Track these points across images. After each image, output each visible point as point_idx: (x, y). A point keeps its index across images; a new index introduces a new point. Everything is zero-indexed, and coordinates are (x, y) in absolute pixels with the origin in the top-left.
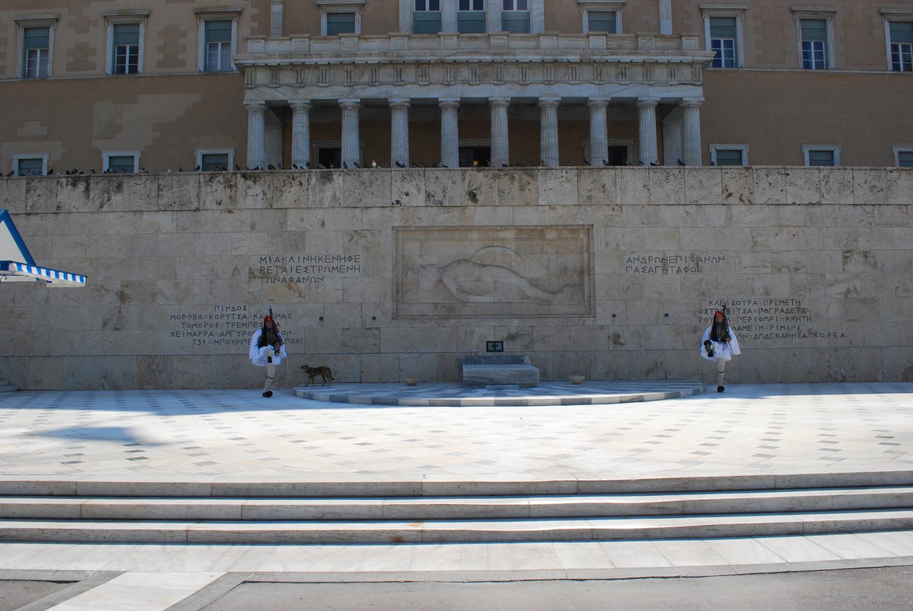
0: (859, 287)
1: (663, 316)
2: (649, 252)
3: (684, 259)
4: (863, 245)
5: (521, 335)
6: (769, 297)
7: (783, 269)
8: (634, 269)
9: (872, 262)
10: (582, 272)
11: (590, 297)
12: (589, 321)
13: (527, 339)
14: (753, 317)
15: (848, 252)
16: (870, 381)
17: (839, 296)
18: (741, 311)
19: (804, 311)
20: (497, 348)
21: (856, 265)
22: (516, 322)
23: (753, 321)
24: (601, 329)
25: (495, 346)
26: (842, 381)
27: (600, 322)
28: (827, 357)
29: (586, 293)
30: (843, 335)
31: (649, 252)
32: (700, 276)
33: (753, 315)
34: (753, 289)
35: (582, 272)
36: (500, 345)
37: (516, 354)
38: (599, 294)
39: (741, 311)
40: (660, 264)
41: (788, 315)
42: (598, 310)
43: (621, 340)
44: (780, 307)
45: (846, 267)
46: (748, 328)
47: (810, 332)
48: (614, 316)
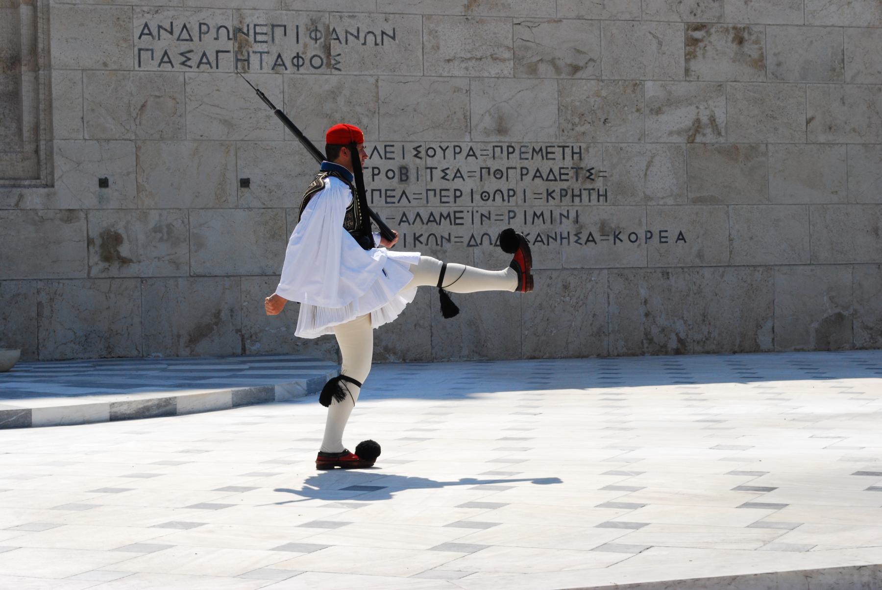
0: (721, 119)
1: (235, 184)
2: (199, 9)
3: (291, 32)
4: (734, 11)
6: (506, 140)
7: (542, 68)
8: (158, 55)
9: (755, 55)
10: (14, 61)
11: (36, 129)
12: (34, 198)
14: (466, 190)
15: (699, 27)
16: (742, 351)
17: (675, 139)
18: (438, 174)
19: (590, 175)
21: (718, 62)
23: (466, 198)
26: (678, 352)
27: (65, 201)
28: (643, 292)
29: (27, 119)
30: (681, 237)
31: (199, 9)
32: (333, 79)
33: (467, 185)
34: (467, 118)
35: (14, 61)
38: (64, 122)
39: (438, 174)
40: (230, 45)
41: (552, 186)
42: (61, 165)
43: (124, 250)
44: (532, 165)
45: (694, 65)
46: (454, 218)
47: (604, 229)
48: (104, 183)
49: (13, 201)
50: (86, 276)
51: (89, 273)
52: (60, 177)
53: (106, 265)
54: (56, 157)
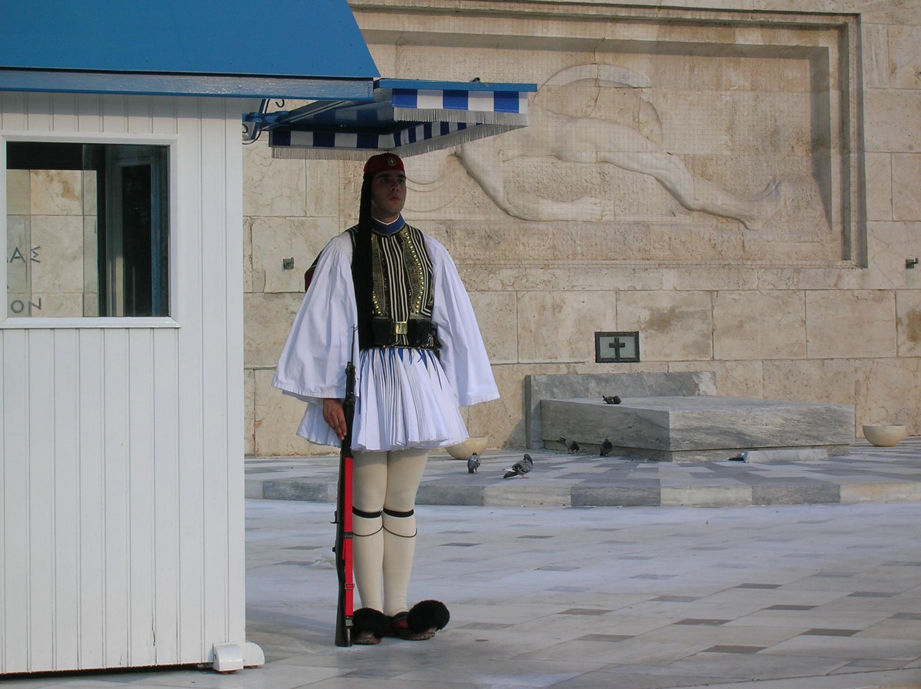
5: (682, 316)
12: (851, 278)
13: (699, 325)
20: (625, 353)
22: (670, 278)
24: (879, 300)
25: (617, 346)
36: (629, 342)
37: (675, 368)
49: (832, 281)
50: (895, 354)
51: (897, 352)
52: (873, 258)
53: (912, 344)
54: (869, 238)
